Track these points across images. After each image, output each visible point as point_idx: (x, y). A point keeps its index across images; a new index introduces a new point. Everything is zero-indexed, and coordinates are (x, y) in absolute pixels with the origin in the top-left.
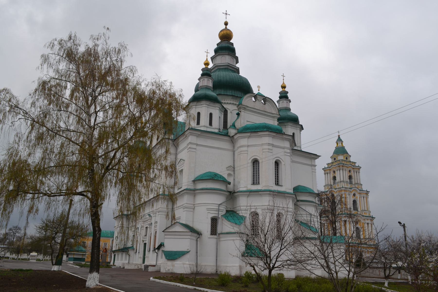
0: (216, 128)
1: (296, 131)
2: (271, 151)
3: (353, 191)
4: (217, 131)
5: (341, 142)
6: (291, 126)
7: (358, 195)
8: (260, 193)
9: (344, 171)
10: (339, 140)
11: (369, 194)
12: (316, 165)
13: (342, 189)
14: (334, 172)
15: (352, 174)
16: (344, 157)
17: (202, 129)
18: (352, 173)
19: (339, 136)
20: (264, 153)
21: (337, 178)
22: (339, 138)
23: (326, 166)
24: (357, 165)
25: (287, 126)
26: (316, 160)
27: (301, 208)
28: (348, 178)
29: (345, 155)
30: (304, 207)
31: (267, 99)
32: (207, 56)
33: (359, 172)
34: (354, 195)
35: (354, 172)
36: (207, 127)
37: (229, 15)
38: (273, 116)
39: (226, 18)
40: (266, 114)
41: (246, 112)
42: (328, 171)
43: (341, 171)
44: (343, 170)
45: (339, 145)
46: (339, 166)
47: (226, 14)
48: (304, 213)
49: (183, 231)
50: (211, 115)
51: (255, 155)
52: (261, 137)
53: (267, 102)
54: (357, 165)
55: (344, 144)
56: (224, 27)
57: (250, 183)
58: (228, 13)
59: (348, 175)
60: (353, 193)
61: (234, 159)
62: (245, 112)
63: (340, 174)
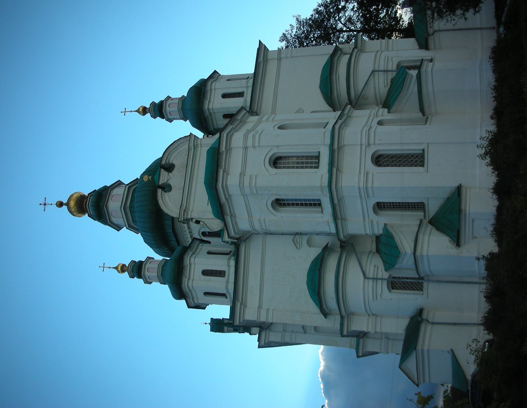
0: (229, 266)
2: (254, 177)
4: (232, 263)
6: (209, 102)
8: (336, 201)
17: (231, 287)
20: (259, 192)
25: (211, 111)
27: (361, 93)
30: (361, 86)
32: (110, 268)
36: (228, 282)
37: (45, 199)
38: (194, 148)
39: (51, 204)
40: (190, 165)
41: (191, 208)
47: (45, 204)
48: (371, 83)
49: (415, 358)
50: (206, 273)
51: (266, 206)
52: (230, 196)
53: (169, 161)
56: (65, 207)
57: (320, 215)
58: (42, 202)
61: (279, 234)
62: (192, 210)
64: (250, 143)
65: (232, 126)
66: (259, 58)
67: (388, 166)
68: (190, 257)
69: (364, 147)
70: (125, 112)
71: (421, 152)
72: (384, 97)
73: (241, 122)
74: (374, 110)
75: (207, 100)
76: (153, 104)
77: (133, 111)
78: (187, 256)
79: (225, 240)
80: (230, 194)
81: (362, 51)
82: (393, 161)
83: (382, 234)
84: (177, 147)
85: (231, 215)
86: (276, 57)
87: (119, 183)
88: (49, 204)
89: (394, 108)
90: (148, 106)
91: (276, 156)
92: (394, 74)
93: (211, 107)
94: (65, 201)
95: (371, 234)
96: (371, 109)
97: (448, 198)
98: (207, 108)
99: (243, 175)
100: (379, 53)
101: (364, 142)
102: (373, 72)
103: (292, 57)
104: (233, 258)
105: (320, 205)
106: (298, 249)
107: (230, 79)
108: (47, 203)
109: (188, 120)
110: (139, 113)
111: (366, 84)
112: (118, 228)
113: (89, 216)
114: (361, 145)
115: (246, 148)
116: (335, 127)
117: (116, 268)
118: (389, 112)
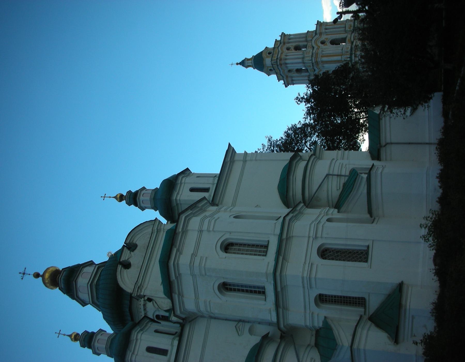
0: (172, 345)
1: (187, 183)
2: (205, 258)
3: (317, 45)
4: (176, 343)
5: (246, 62)
6: (178, 194)
7: (323, 38)
8: (279, 289)
9: (288, 57)
10: (243, 63)
11: (322, 22)
12: (245, 151)
13: (314, 61)
14: (290, 71)
15: (292, 46)
16: (267, 57)
18: (292, 45)
19: (237, 64)
21: (299, 68)
22: (240, 64)
23: (282, 82)
24: (279, 39)
25: (178, 202)
26: (238, 151)
28: (298, 51)
29: (264, 55)
30: (315, 188)
31: (128, 242)
32: (64, 335)
33: (290, 35)
34: (323, 43)
35: (289, 43)
37: (25, 268)
38: (157, 232)
39: (29, 274)
41: (145, 287)
42: (290, 79)
43: (288, 61)
44: (286, 59)
45: (251, 64)
46: (281, 65)
47: (24, 274)
48: (325, 187)
50: (150, 350)
52: (180, 274)
53: (133, 241)
54: (279, 39)
55: (250, 57)
56: (40, 278)
57: (263, 302)
58: (22, 271)
59: (294, 51)
60: (320, 45)
61: (223, 319)
62: (146, 288)
63: (292, 63)
64: (205, 227)
65: (191, 211)
66: (227, 158)
67: (333, 259)
68: (137, 333)
69: (311, 239)
70: (105, 197)
71: (366, 248)
72: (335, 201)
73: (201, 209)
74: (324, 210)
75: (176, 191)
76: (130, 192)
77: (112, 197)
78: (135, 332)
79: (172, 319)
80: (180, 273)
81: (320, 158)
82: (338, 256)
83: (322, 327)
84: (142, 229)
85: (179, 294)
86: (242, 159)
87: (91, 263)
88: (27, 274)
89: (343, 209)
90: (125, 194)
91: (228, 241)
92: (347, 178)
93: (178, 198)
94: (41, 274)
95: (311, 326)
96: (322, 209)
97: (389, 295)
98: (175, 198)
99: (194, 256)
100: (334, 161)
101: (311, 235)
102: (328, 175)
103: (256, 160)
104: (178, 338)
105: (264, 293)
106: (239, 336)
107: (200, 176)
108: (26, 273)
109: (158, 211)
110: (117, 199)
111: (320, 186)
112: (84, 304)
113: (59, 289)
114: (309, 237)
115: (201, 231)
116: (286, 218)
117: (70, 336)
118: (338, 212)
